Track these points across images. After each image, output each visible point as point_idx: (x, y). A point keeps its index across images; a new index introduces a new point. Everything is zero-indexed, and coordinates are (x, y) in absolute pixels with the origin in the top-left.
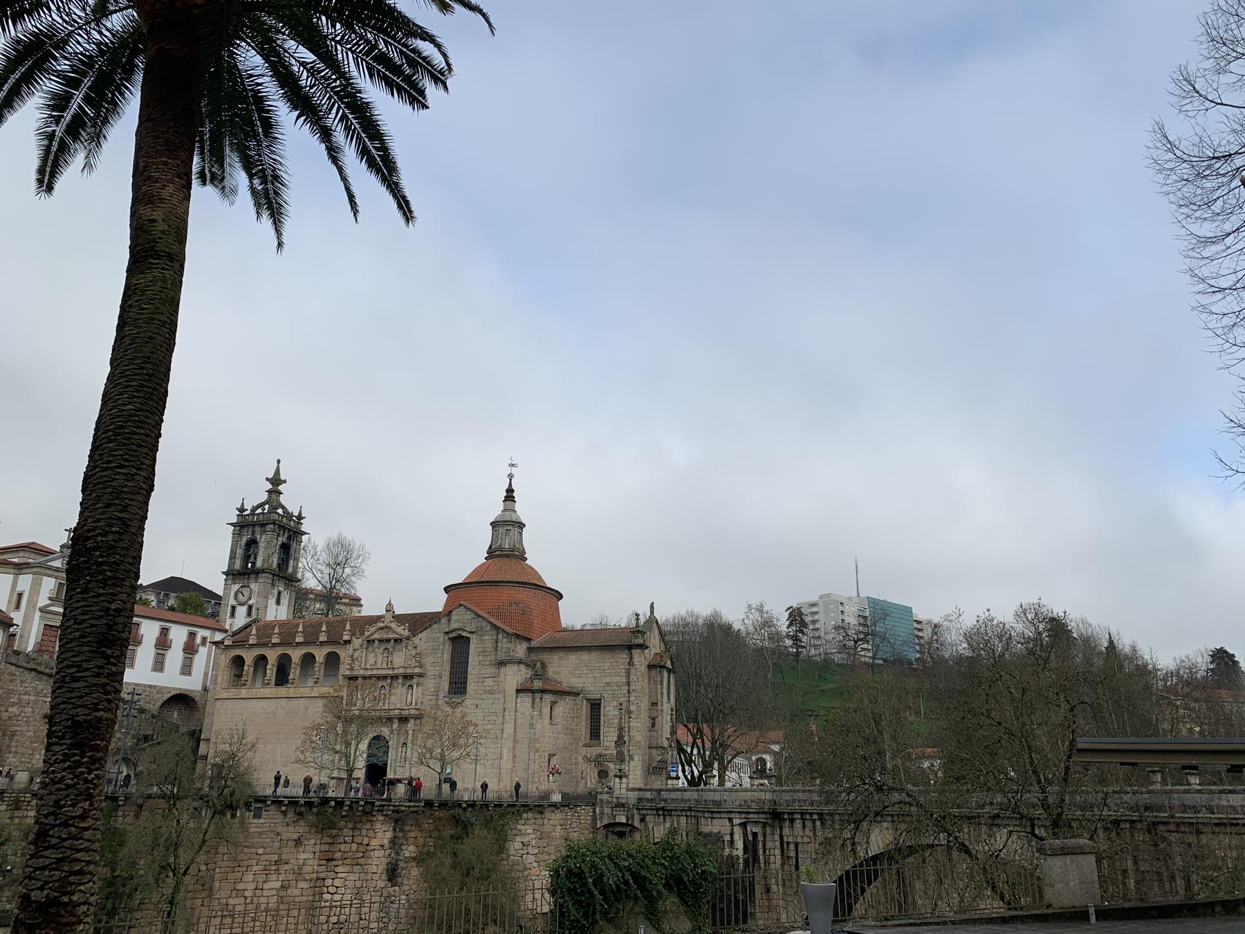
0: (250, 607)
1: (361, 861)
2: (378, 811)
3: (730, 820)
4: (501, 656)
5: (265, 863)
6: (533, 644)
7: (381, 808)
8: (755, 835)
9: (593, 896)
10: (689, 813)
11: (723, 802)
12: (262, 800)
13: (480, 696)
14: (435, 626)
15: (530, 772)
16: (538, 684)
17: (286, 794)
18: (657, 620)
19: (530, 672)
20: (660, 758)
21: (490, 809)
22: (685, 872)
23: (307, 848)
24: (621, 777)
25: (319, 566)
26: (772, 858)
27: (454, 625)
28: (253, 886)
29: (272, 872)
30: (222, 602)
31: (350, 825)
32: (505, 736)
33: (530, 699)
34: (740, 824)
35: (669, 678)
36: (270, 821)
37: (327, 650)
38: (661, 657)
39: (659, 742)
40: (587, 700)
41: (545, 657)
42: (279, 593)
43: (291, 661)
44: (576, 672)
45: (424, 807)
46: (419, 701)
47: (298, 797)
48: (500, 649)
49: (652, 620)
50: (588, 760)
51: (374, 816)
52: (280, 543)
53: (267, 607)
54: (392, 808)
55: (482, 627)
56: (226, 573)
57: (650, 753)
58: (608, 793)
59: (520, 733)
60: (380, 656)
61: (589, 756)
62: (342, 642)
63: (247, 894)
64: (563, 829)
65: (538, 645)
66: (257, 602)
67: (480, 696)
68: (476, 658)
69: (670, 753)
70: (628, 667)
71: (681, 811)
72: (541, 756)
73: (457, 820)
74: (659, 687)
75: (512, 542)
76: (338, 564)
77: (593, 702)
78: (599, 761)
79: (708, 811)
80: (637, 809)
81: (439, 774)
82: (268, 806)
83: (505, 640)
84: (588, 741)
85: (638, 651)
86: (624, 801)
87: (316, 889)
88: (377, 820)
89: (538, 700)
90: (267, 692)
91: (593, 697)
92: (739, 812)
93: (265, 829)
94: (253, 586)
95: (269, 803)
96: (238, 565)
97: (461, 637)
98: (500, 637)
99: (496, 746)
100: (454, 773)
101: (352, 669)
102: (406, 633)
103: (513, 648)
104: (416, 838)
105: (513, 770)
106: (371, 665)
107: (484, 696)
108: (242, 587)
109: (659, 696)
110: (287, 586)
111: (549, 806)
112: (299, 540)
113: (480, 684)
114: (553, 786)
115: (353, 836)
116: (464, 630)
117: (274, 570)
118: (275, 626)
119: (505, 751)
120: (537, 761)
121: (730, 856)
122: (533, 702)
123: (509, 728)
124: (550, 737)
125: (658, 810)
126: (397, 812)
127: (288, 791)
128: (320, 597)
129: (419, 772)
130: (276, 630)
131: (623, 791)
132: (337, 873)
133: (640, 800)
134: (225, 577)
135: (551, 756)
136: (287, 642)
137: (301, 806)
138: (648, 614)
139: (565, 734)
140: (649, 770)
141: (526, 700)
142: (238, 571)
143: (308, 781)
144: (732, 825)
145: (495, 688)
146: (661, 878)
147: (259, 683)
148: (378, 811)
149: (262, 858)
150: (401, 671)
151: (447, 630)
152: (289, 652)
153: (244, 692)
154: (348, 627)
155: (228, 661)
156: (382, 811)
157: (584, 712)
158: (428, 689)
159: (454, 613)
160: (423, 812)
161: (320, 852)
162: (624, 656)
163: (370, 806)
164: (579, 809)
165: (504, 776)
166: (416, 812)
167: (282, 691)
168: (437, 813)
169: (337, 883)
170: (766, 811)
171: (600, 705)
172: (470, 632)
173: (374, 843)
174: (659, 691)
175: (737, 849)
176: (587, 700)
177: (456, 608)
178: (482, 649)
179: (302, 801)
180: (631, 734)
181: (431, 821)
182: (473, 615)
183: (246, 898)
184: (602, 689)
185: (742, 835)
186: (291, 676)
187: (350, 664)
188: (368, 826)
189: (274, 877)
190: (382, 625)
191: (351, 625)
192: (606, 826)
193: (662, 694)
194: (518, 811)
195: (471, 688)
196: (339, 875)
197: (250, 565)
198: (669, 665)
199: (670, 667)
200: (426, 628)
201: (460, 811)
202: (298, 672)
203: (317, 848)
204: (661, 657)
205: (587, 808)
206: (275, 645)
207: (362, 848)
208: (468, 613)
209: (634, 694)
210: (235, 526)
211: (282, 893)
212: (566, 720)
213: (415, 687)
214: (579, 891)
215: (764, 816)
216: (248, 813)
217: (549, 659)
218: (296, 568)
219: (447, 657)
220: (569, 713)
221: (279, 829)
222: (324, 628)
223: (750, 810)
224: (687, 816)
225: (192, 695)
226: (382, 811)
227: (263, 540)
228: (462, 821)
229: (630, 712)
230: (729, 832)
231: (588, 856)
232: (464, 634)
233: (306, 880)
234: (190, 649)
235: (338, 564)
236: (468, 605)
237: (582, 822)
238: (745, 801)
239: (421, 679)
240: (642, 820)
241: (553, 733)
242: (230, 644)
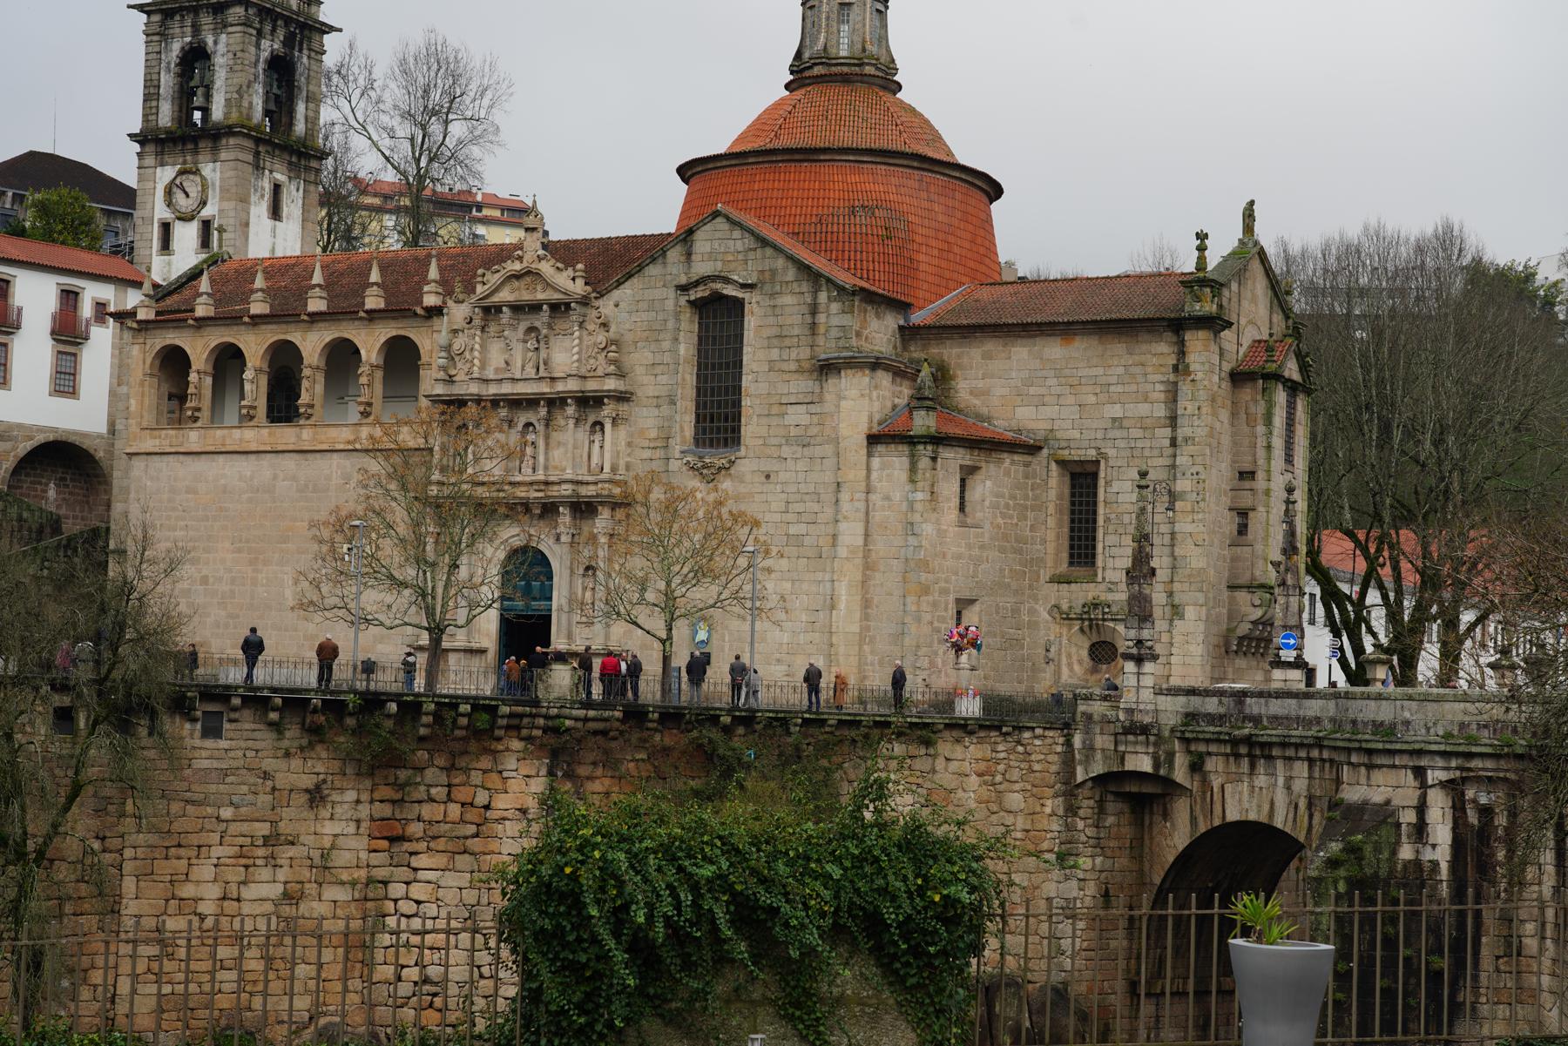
0: (206, 225)
1: (474, 844)
2: (508, 728)
3: (1420, 773)
4: (828, 348)
5: (241, 840)
6: (917, 318)
7: (515, 721)
8: (1486, 812)
9: (605, 957)
10: (1315, 753)
11: (1399, 727)
12: (218, 694)
13: (774, 452)
14: (653, 270)
15: (907, 641)
16: (923, 422)
17: (275, 683)
18: (1262, 255)
19: (906, 391)
20: (1259, 613)
21: (794, 729)
22: (894, 898)
23: (338, 810)
24: (1139, 660)
25: (385, 119)
26: (1531, 872)
27: (701, 268)
28: (214, 891)
29: (259, 862)
30: (137, 214)
31: (441, 761)
32: (842, 552)
33: (905, 461)
34: (1443, 785)
35: (1291, 407)
36: (243, 744)
37: (384, 332)
38: (1270, 349)
39: (1257, 573)
40: (1062, 463)
41: (950, 352)
42: (277, 188)
43: (301, 358)
44: (1032, 390)
45: (623, 721)
46: (622, 463)
47: (308, 691)
48: (822, 330)
49: (1249, 252)
50: (1067, 618)
51: (499, 739)
52: (265, 55)
53: (247, 225)
54: (541, 721)
55: (773, 272)
56: (141, 138)
57: (1232, 601)
58: (1105, 698)
59: (880, 547)
60: (518, 349)
61: (1065, 607)
62: (419, 311)
63: (203, 908)
64: (985, 783)
65: (928, 322)
66: (221, 211)
67: (774, 452)
68: (761, 355)
69: (1281, 600)
70: (1172, 377)
71: (1297, 746)
72: (935, 604)
73: (706, 756)
74: (1261, 429)
75: (857, 39)
76: (434, 113)
77: (1078, 470)
78: (1091, 619)
79: (1359, 750)
80: (1186, 741)
81: (663, 642)
82: (235, 709)
83: (835, 307)
84: (1063, 567)
85: (1202, 334)
86: (1147, 720)
87: (370, 905)
88: (507, 749)
89: (924, 463)
90: (252, 437)
91: (1076, 455)
92: (1445, 755)
93: (235, 764)
94: (208, 170)
95: (236, 701)
96: (166, 116)
97: (718, 297)
98: (823, 297)
99: (819, 576)
100: (715, 642)
101: (450, 380)
102: (579, 288)
103: (856, 327)
104: (607, 794)
105: (864, 636)
106: (497, 370)
107: (786, 451)
108: (181, 173)
109: (1261, 453)
110: (295, 170)
111: (948, 726)
112: (315, 46)
113: (775, 421)
114: (965, 678)
115: (449, 786)
116: (727, 280)
117: (258, 128)
118: (254, 275)
119: (842, 590)
120: (927, 617)
121: (1417, 863)
122: (913, 469)
123: (851, 533)
124: (959, 557)
125: (1235, 742)
126: (556, 731)
127: (281, 677)
128: (387, 201)
129: (619, 637)
130: (259, 282)
131: (1146, 695)
132: (415, 870)
133: (1191, 717)
134: (137, 147)
135: (963, 604)
136: (287, 311)
137: (315, 711)
138: (1238, 232)
139: (1002, 550)
140: (1227, 644)
141: (892, 465)
142: (168, 131)
143: (327, 653)
144: (1424, 786)
145: (814, 431)
146: (823, 915)
147: (231, 415)
148: (508, 728)
149: (234, 828)
150: (573, 385)
151: (683, 280)
152: (295, 337)
153: (193, 438)
154: (433, 273)
155: (149, 361)
156: (518, 728)
157: (1052, 494)
158: (642, 432)
159: (699, 235)
160: (622, 733)
161: (372, 819)
162: (1161, 350)
163: (485, 717)
164: (1027, 735)
165: (842, 650)
166: (604, 733)
167: (286, 435)
168: (658, 737)
169: (417, 891)
170: (1520, 751)
171: (1095, 475)
172: (744, 286)
173: (501, 802)
174: (1261, 442)
175: (1434, 846)
176: (1062, 463)
177: (703, 223)
178: (775, 331)
179: (316, 701)
180: (1178, 552)
181: (643, 756)
182: (749, 242)
183: (202, 918)
184: (1100, 435)
185: (1449, 812)
186: (304, 398)
187: (444, 368)
188: (485, 762)
189: (265, 874)
190: (517, 266)
191: (441, 269)
192: (1099, 780)
193: (1269, 447)
194: (866, 736)
195: (751, 428)
196: (422, 875)
197: (197, 115)
198: (1292, 370)
199: (1296, 377)
200: (629, 276)
201: (715, 734)
202: (319, 388)
203: (364, 811)
204: (1270, 349)
205: (1051, 733)
206: (257, 320)
207: (471, 815)
208: (737, 234)
209: (1191, 449)
210: (149, 13)
211: (287, 910)
212: (1003, 516)
213: (608, 427)
214: (571, 938)
215: (1512, 764)
216: (188, 726)
217: (959, 357)
218: (312, 121)
219: (686, 348)
220: (1013, 497)
221: (269, 764)
222: (375, 276)
223: (1474, 749)
224: (1311, 761)
225: (86, 444)
226: (518, 728)
227: (222, 46)
228: (722, 758)
229: (1173, 496)
230: (1415, 802)
231: (595, 846)
232: (730, 291)
233: (343, 883)
234: (68, 332)
235: (434, 113)
236: (735, 214)
237: (1037, 767)
238: (1462, 726)
239: (624, 407)
240: (1196, 767)
241: (969, 547)
242: (152, 316)
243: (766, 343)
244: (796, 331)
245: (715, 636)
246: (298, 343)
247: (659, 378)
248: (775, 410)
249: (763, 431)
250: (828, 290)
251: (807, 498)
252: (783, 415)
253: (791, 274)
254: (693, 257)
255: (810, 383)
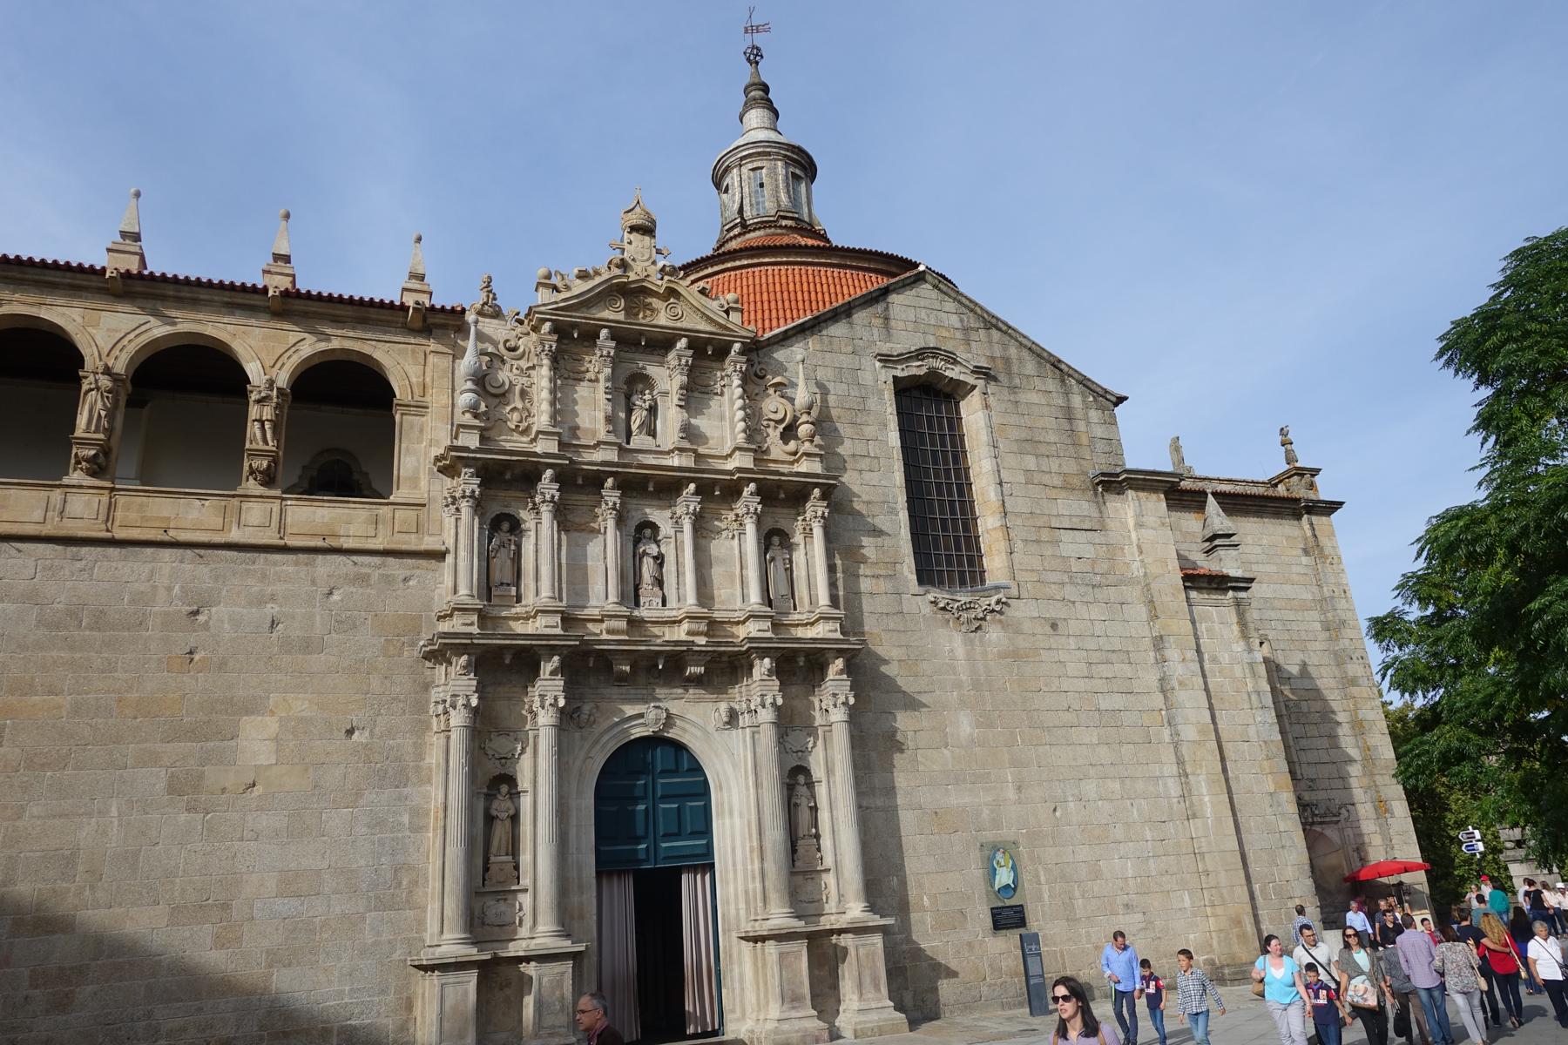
13: (1053, 590)
48: (1085, 441)
107: (1070, 592)
113: (1048, 551)
145: (1103, 567)
208: (950, 305)
232: (953, 373)
243: (1015, 448)
244: (1052, 438)
245: (1026, 877)
246: (70, 328)
247: (867, 476)
248: (1045, 535)
249: (1036, 563)
250: (1082, 394)
251: (1114, 657)
252: (1056, 543)
253: (1030, 367)
254: (893, 323)
255: (1085, 505)
